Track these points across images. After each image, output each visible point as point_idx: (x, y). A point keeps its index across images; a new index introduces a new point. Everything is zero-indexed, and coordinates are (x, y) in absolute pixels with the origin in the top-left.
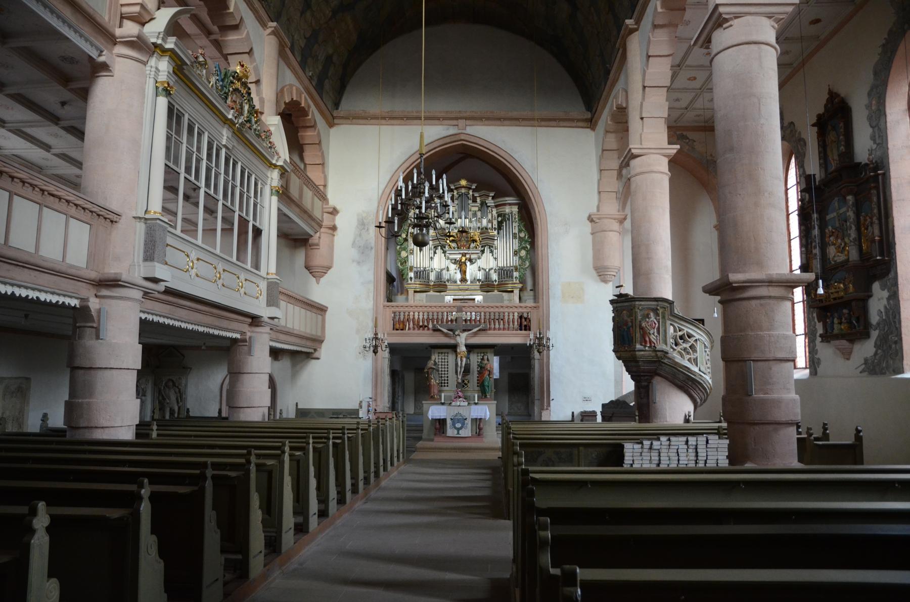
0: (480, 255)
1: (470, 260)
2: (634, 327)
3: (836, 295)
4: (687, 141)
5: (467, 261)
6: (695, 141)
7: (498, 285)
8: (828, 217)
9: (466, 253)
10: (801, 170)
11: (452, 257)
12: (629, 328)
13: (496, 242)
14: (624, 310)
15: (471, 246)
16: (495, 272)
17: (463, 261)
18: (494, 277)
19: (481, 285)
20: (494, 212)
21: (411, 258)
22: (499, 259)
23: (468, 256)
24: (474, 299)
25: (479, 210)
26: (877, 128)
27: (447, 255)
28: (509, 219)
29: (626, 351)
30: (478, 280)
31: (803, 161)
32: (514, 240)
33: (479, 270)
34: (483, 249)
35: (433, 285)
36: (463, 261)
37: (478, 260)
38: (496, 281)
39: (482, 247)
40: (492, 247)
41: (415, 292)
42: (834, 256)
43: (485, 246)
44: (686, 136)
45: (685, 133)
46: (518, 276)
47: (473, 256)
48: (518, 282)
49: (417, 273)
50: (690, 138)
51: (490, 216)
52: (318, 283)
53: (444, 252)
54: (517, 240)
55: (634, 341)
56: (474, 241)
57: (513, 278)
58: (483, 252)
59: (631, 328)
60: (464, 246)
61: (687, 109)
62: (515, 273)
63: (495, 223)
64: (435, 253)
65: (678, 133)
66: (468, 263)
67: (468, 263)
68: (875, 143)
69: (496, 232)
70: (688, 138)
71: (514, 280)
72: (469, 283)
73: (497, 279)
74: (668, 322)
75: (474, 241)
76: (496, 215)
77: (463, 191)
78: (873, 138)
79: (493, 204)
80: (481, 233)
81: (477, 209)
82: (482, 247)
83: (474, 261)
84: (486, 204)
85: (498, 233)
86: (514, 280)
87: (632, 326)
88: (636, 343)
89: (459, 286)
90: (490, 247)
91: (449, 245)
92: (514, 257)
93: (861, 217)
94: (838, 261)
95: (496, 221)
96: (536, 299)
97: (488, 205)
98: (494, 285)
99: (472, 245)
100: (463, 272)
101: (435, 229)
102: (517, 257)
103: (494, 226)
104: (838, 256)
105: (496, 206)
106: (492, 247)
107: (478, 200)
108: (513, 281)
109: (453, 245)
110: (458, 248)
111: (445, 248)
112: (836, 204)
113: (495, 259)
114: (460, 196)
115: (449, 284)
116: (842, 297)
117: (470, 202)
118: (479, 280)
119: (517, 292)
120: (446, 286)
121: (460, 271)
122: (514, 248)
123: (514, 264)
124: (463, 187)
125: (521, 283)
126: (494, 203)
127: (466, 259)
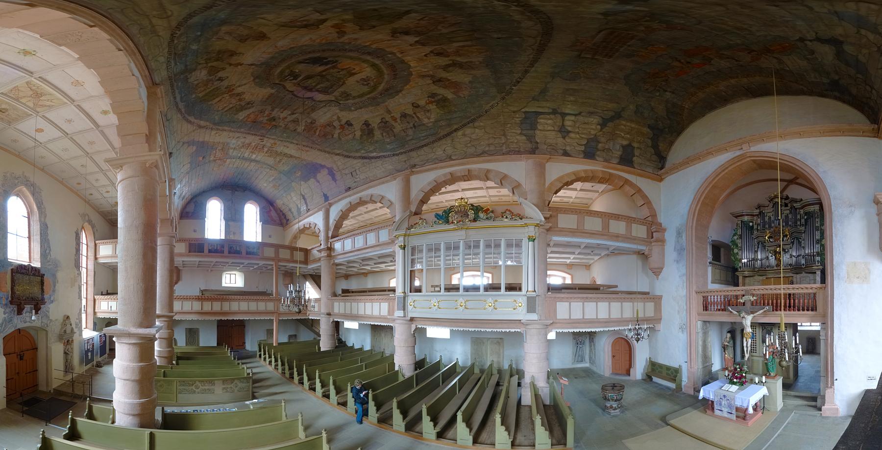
7: (805, 267)
15: (785, 240)
16: (803, 258)
18: (803, 262)
25: (791, 213)
27: (767, 248)
28: (813, 217)
30: (789, 265)
32: (817, 232)
38: (803, 264)
39: (792, 239)
43: (794, 238)
46: (819, 260)
48: (819, 264)
52: (658, 279)
54: (819, 232)
58: (793, 243)
63: (803, 221)
69: (804, 227)
71: (817, 263)
76: (804, 215)
81: (788, 212)
83: (786, 250)
85: (805, 228)
86: (817, 263)
89: (775, 270)
90: (798, 239)
92: (817, 245)
96: (823, 280)
100: (778, 260)
101: (758, 230)
102: (819, 245)
103: (802, 223)
106: (801, 239)
107: (789, 205)
108: (815, 264)
114: (774, 205)
119: (819, 273)
125: (821, 265)
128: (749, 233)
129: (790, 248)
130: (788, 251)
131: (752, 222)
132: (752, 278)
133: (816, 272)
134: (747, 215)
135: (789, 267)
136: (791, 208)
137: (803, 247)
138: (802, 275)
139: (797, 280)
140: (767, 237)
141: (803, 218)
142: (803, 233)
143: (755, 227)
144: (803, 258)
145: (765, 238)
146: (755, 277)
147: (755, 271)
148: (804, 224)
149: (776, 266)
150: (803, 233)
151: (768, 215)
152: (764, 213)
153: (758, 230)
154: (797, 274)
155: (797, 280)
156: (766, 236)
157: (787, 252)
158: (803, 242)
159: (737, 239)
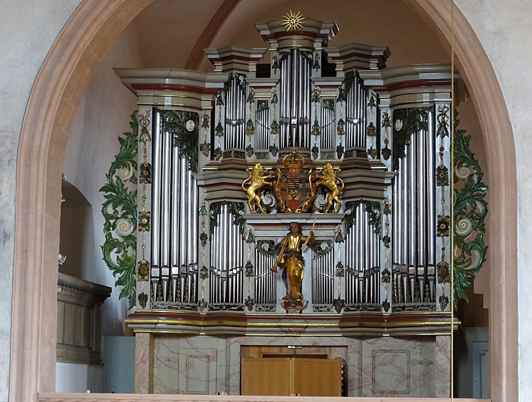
0: (342, 228)
1: (314, 244)
5: (304, 246)
7: (392, 318)
9: (300, 225)
11: (261, 234)
13: (388, 193)
15: (317, 204)
17: (292, 247)
19: (342, 319)
20: (386, 101)
21: (143, 237)
22: (398, 242)
23: (306, 233)
24: (325, 357)
25: (343, 97)
27: (248, 228)
33: (339, 275)
34: (349, 212)
35: (207, 318)
36: (292, 247)
37: (336, 245)
38: (386, 305)
40: (378, 206)
41: (155, 336)
43: (357, 204)
47: (321, 234)
49: (160, 282)
51: (372, 119)
53: (240, 221)
56: (325, 190)
57: (434, 301)
58: (349, 220)
60: (295, 205)
62: (439, 286)
63: (386, 133)
64: (213, 223)
66: (308, 255)
67: (308, 255)
69: (390, 160)
72: (308, 311)
73: (390, 301)
75: (325, 190)
76: (390, 113)
77: (296, 42)
79: (380, 83)
80: (344, 167)
81: (335, 94)
82: (348, 206)
83: (324, 246)
84: (361, 81)
85: (395, 166)
89: (280, 318)
91: (255, 201)
92: (439, 239)
95: (390, 129)
97: (366, 83)
98: (381, 318)
99: (320, 201)
101: (214, 153)
103: (383, 145)
105: (389, 88)
106: (378, 206)
107: (340, 67)
109: (266, 200)
110: (279, 211)
111: (242, 207)
113: (386, 240)
115: (253, 313)
117: (317, 73)
118: (338, 304)
120: (244, 318)
121: (284, 276)
122: (439, 212)
123: (439, 261)
124: (293, 33)
126: (384, 79)
127: (301, 243)
128: (180, 157)
129: (339, 240)
130: (331, 249)
131: (195, 118)
132: (183, 342)
133: (433, 338)
134: (173, 88)
135: (334, 312)
136: (349, 80)
137: (386, 240)
138: (380, 343)
139: (360, 363)
140: (251, 190)
141: (386, 125)
142: (388, 185)
143: (204, 136)
144: (386, 280)
145: (246, 192)
146: (193, 339)
147: (198, 317)
148: (390, 147)
149: (286, 305)
150: (388, 185)
151: (260, 95)
152: (243, 89)
153: (214, 153)
154: (362, 338)
155: (360, 363)
156: (247, 186)
157: (324, 253)
158: (384, 216)
159: (133, 179)
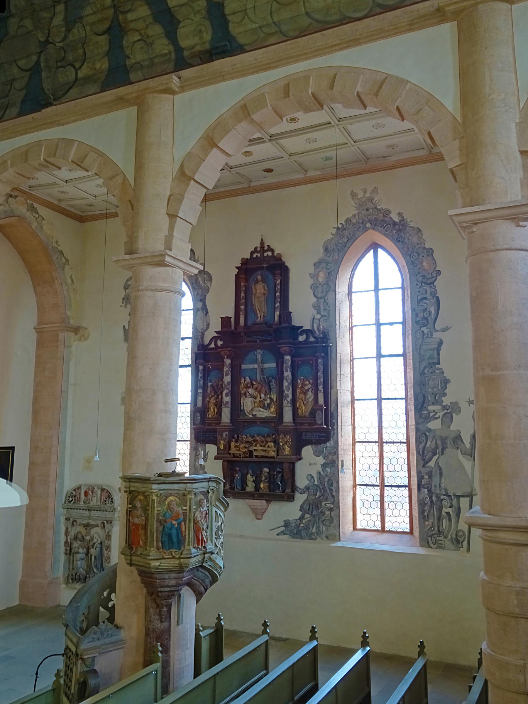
2: (188, 521)
3: (263, 454)
4: (37, 216)
6: (44, 220)
8: (244, 366)
10: (200, 305)
12: (179, 524)
14: (171, 495)
26: (323, 300)
29: (174, 557)
31: (205, 296)
42: (252, 410)
44: (36, 209)
45: (35, 205)
50: (40, 214)
55: (187, 544)
59: (183, 523)
61: (66, 182)
65: (29, 202)
68: (319, 312)
70: (38, 213)
74: (215, 509)
78: (317, 308)
87: (185, 520)
88: (189, 545)
93: (299, 381)
94: (258, 416)
104: (260, 411)
112: (259, 356)
116: (274, 458)
